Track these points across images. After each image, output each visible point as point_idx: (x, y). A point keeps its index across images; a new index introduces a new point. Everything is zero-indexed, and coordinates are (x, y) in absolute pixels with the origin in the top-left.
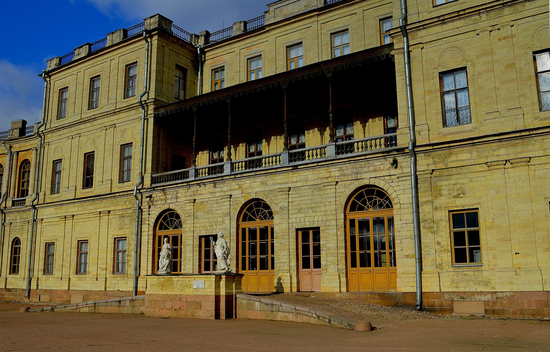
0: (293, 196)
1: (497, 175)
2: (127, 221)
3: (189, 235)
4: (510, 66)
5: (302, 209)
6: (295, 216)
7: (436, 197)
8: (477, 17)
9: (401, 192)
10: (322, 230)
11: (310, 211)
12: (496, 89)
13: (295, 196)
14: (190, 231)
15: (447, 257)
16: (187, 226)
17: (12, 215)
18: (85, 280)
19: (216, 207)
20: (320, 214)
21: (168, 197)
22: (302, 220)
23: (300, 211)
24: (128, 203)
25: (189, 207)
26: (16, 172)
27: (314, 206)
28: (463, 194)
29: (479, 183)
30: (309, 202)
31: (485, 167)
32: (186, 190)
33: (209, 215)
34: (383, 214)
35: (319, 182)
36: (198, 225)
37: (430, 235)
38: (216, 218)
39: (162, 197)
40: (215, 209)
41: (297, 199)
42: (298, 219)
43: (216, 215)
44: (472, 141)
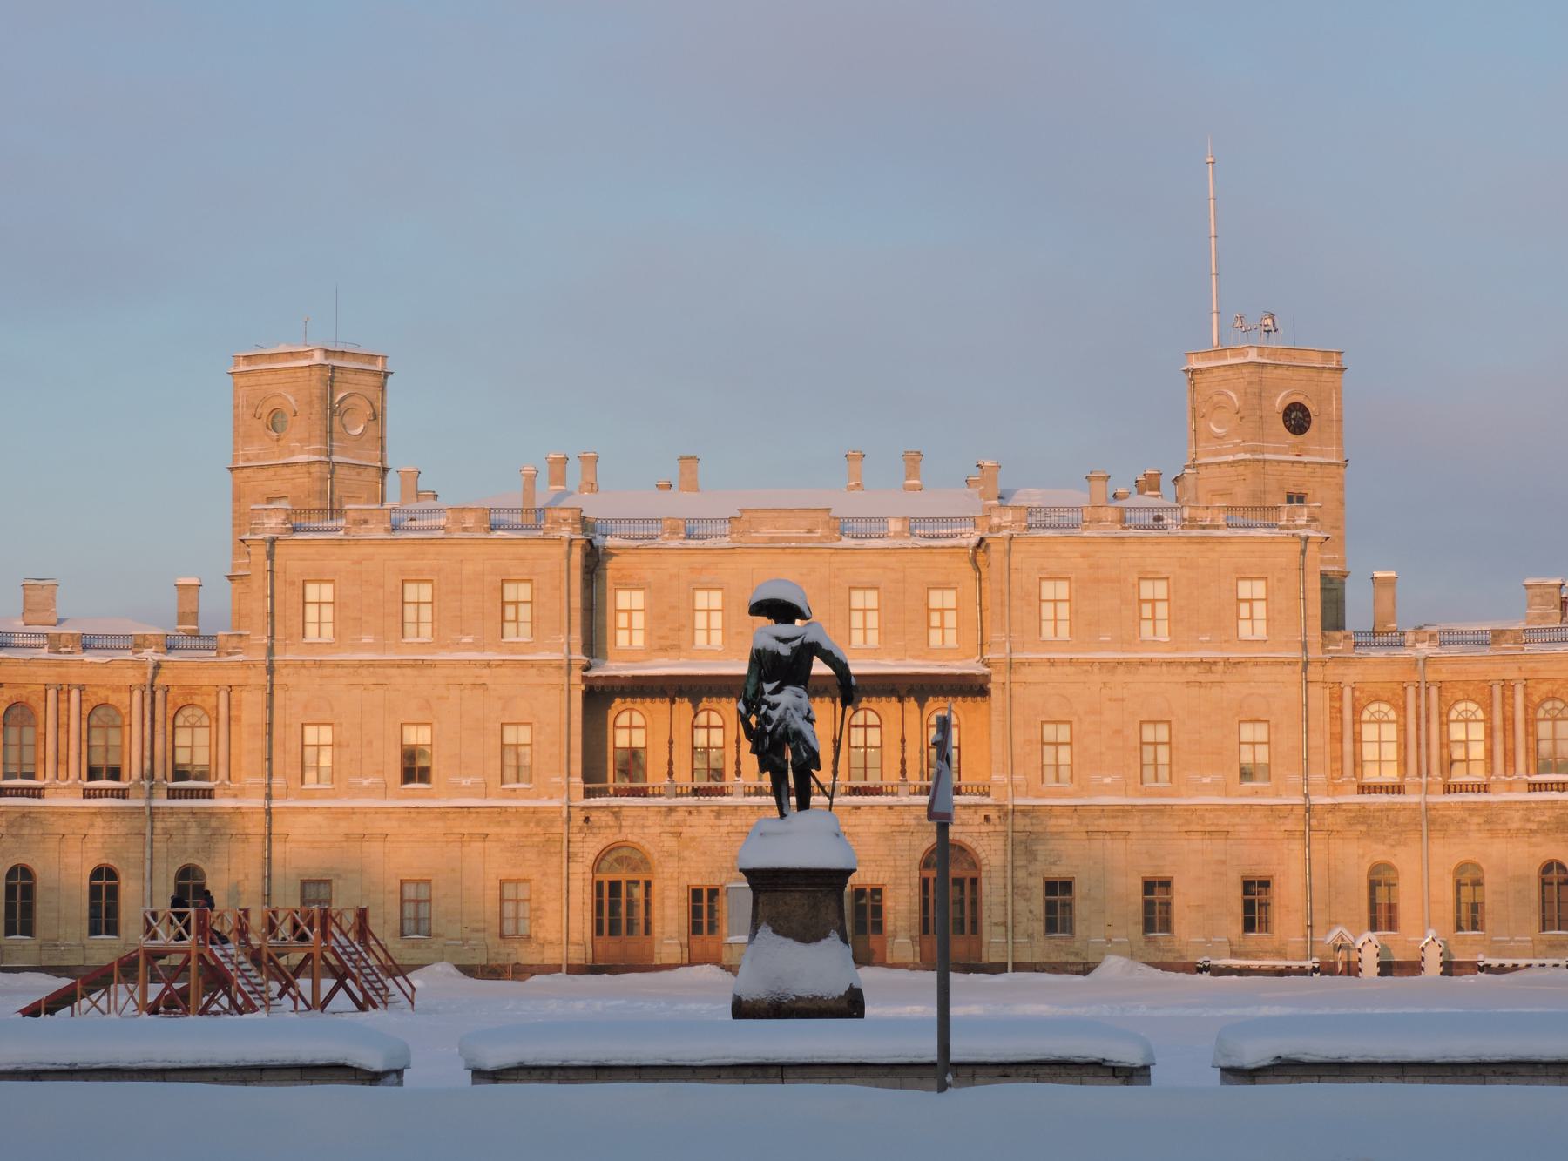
4: (1118, 732)
7: (1030, 862)
8: (1089, 668)
9: (993, 852)
11: (874, 864)
12: (1101, 753)
14: (672, 878)
15: (1039, 926)
16: (666, 870)
17: (173, 819)
18: (429, 948)
20: (886, 869)
21: (624, 823)
24: (532, 825)
25: (669, 842)
26: (165, 727)
31: (1084, 836)
32: (662, 818)
35: (888, 829)
36: (686, 870)
39: (611, 823)
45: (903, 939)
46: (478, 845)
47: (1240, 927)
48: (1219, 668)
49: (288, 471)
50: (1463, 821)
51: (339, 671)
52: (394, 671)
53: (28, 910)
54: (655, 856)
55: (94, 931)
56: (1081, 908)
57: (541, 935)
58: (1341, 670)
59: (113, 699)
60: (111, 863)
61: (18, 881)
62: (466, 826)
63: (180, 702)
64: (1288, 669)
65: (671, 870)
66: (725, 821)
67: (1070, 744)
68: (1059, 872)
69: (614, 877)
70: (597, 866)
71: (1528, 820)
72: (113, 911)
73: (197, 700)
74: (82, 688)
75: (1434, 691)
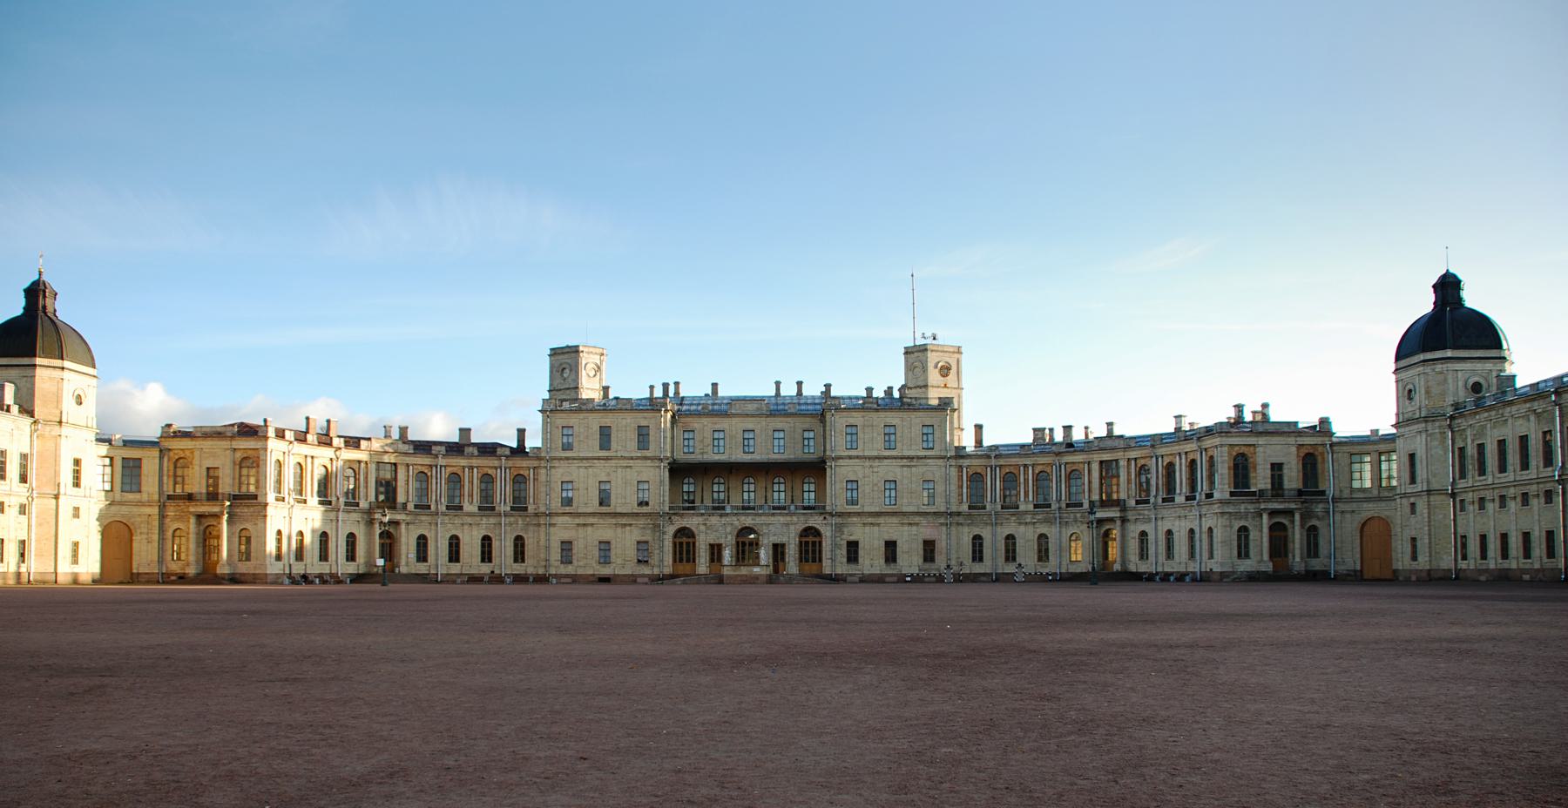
1: (867, 528)
2: (649, 531)
4: (876, 485)
15: (845, 560)
23: (774, 535)
25: (702, 528)
34: (817, 539)
44: (858, 514)
45: (792, 564)
46: (628, 528)
47: (921, 560)
48: (915, 460)
49: (568, 392)
50: (1008, 519)
51: (575, 461)
52: (596, 461)
53: (458, 552)
55: (483, 560)
56: (861, 553)
57: (653, 562)
58: (961, 461)
59: (490, 472)
60: (489, 534)
61: (455, 541)
62: (624, 521)
63: (515, 474)
64: (942, 460)
66: (723, 519)
67: (857, 489)
68: (852, 538)
69: (681, 540)
70: (675, 536)
71: (1034, 519)
72: (490, 553)
73: (522, 473)
74: (476, 467)
75: (998, 469)
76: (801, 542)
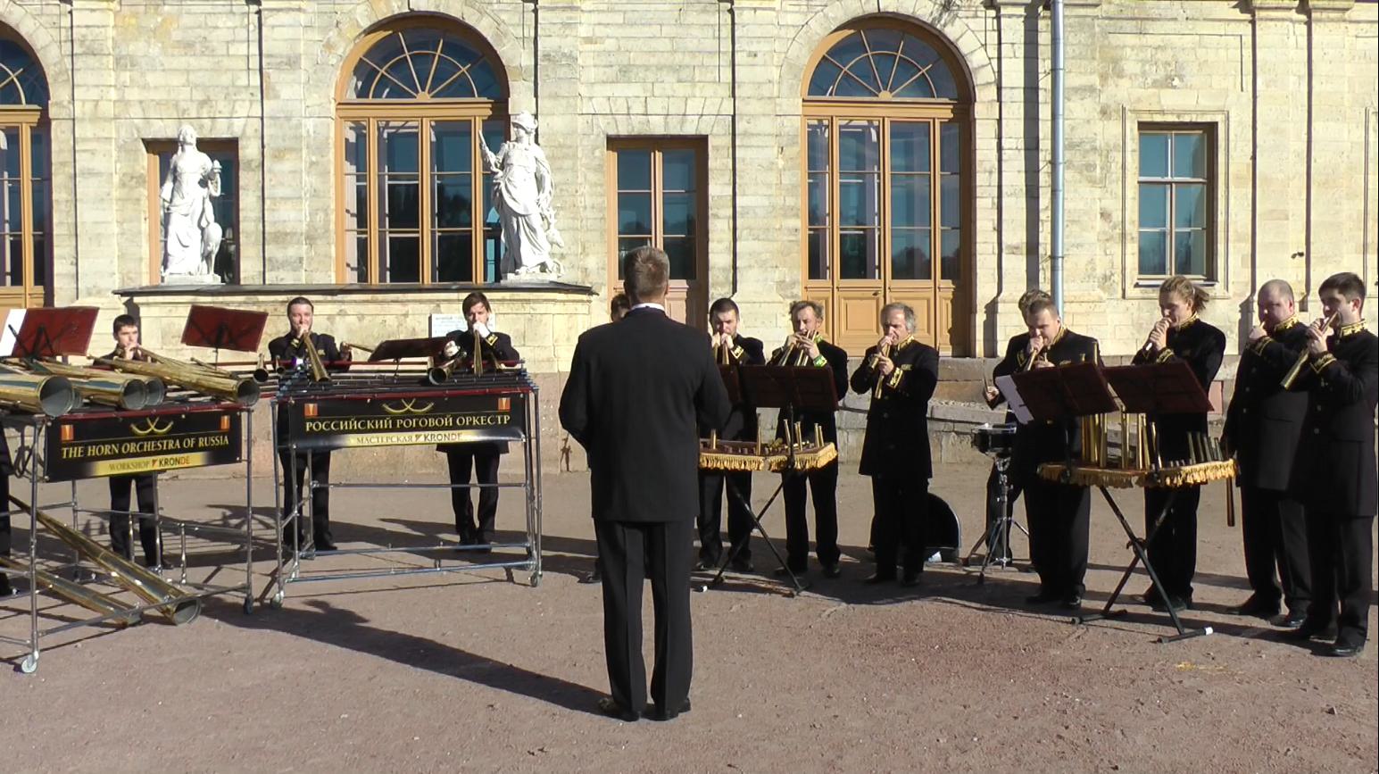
0: (594, 18)
3: (90, 135)
5: (635, 70)
6: (608, 90)
10: (716, 148)
11: (670, 78)
13: (604, 18)
14: (95, 119)
19: (225, 30)
20: (709, 90)
22: (637, 108)
23: (625, 72)
27: (687, 60)
28: (1181, 78)
29: (1222, 53)
30: (664, 45)
33: (192, 60)
36: (133, 94)
37: (1085, 190)
38: (229, 75)
40: (223, 34)
41: (609, 31)
42: (621, 102)
43: (226, 62)
54: (50, 56)
65: (94, 94)
68: (1179, 104)
76: (813, 134)
